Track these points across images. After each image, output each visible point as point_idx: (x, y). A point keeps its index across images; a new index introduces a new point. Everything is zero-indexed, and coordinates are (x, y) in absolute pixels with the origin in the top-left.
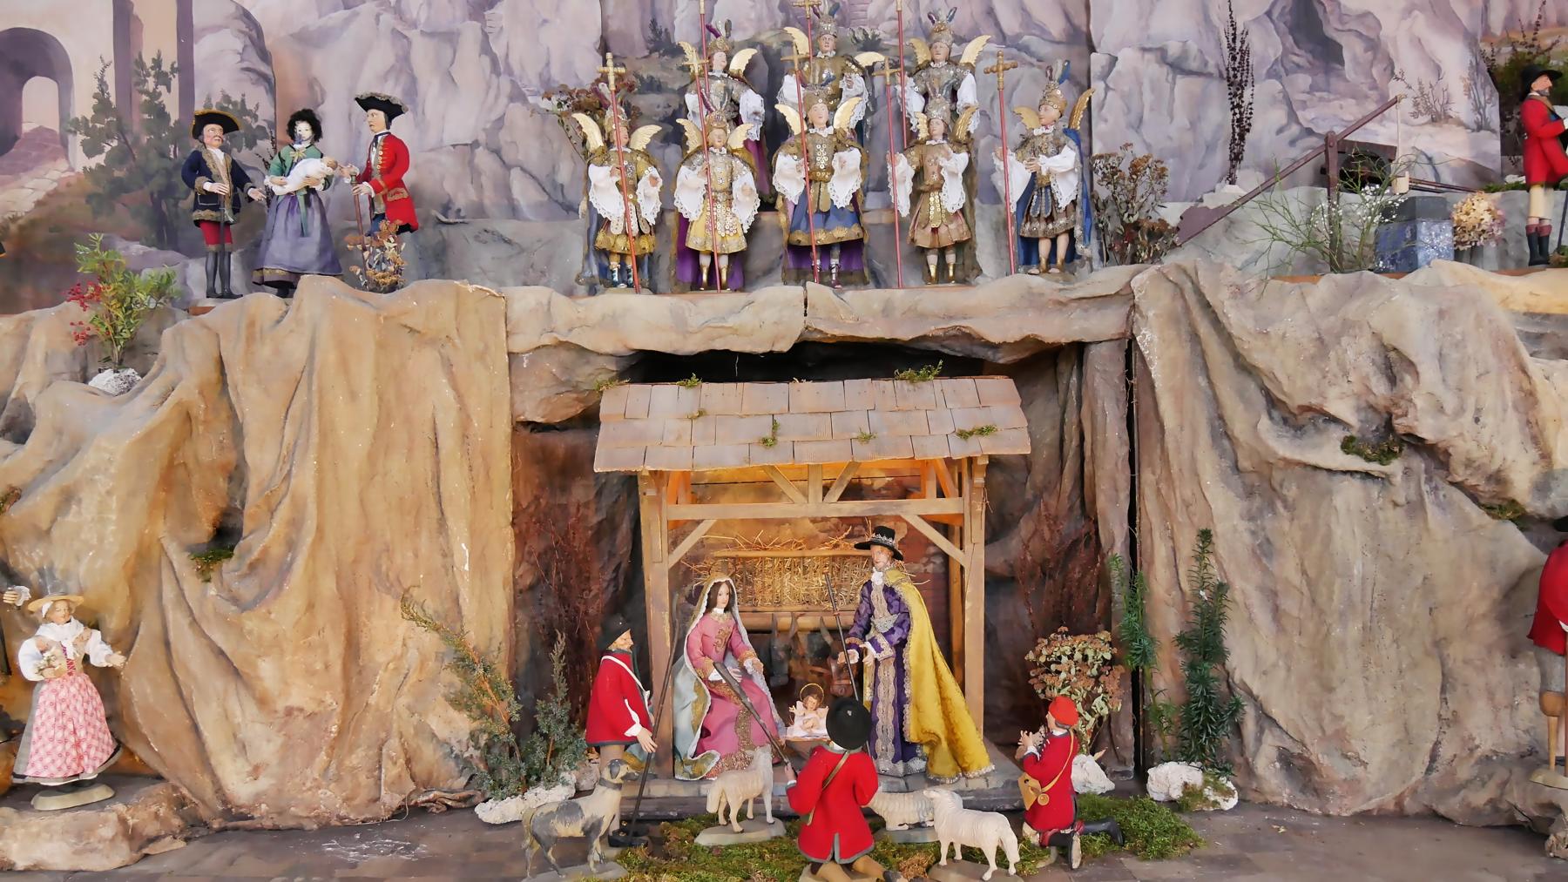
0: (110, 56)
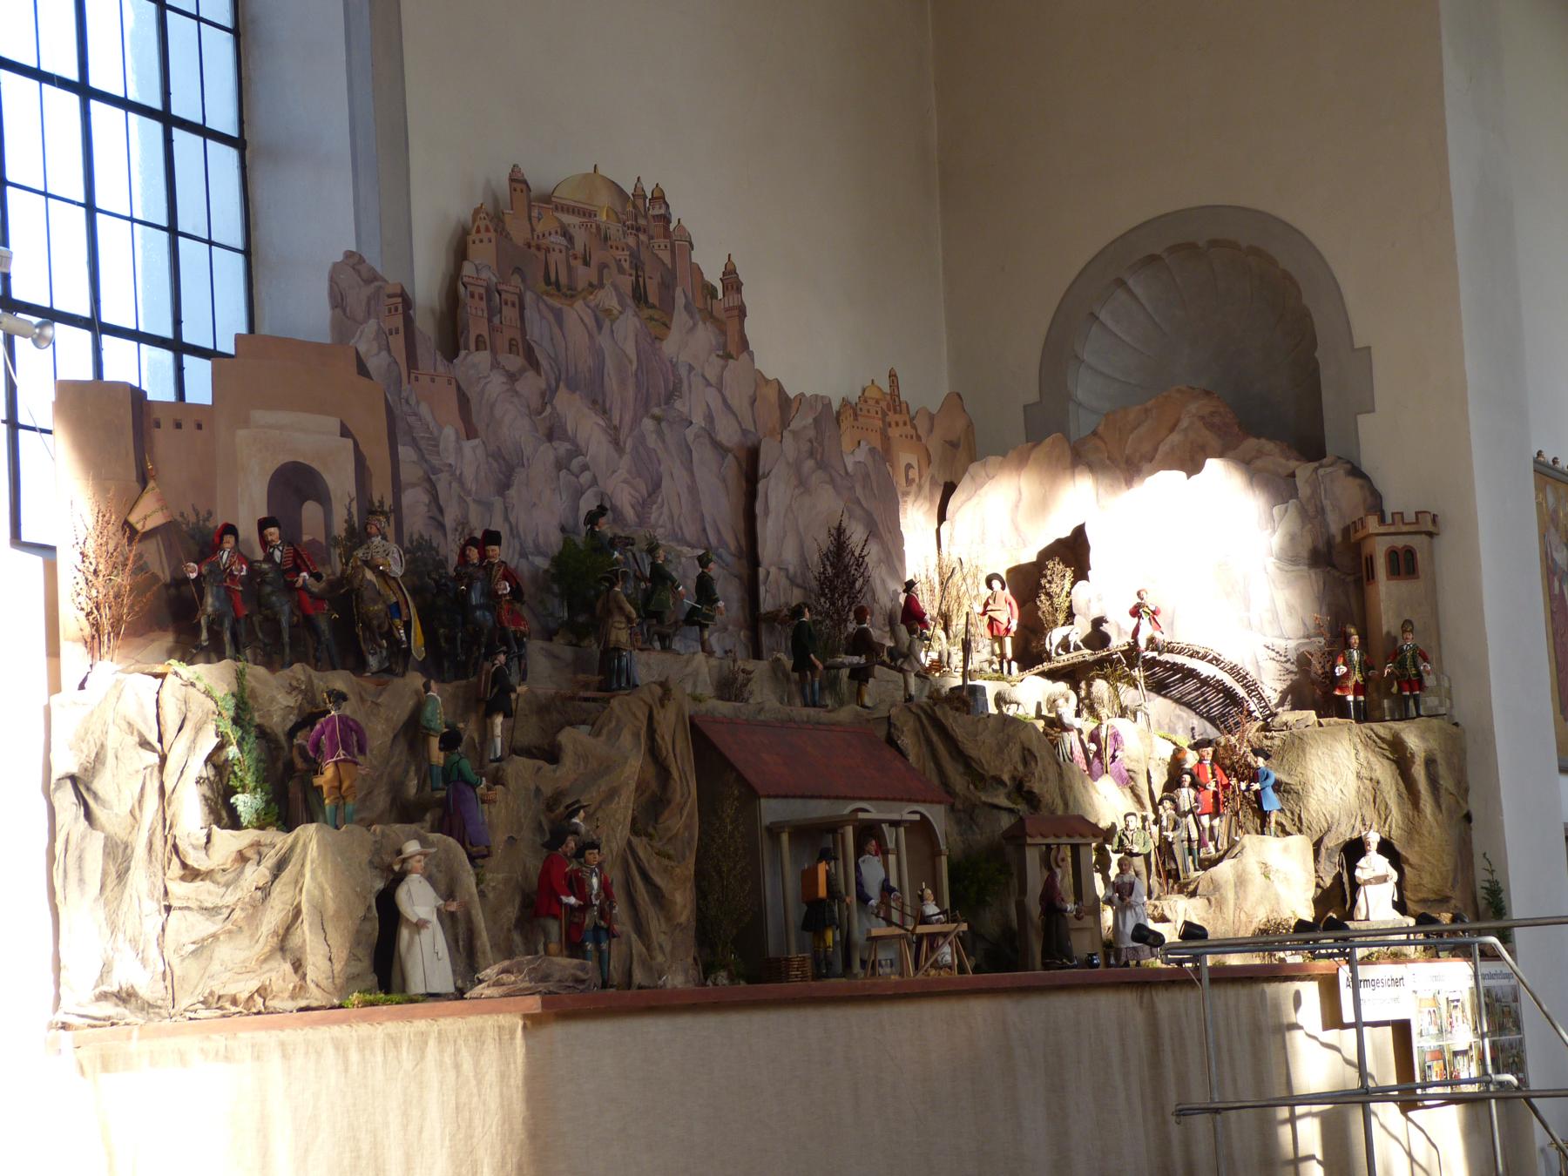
0: (354, 494)
